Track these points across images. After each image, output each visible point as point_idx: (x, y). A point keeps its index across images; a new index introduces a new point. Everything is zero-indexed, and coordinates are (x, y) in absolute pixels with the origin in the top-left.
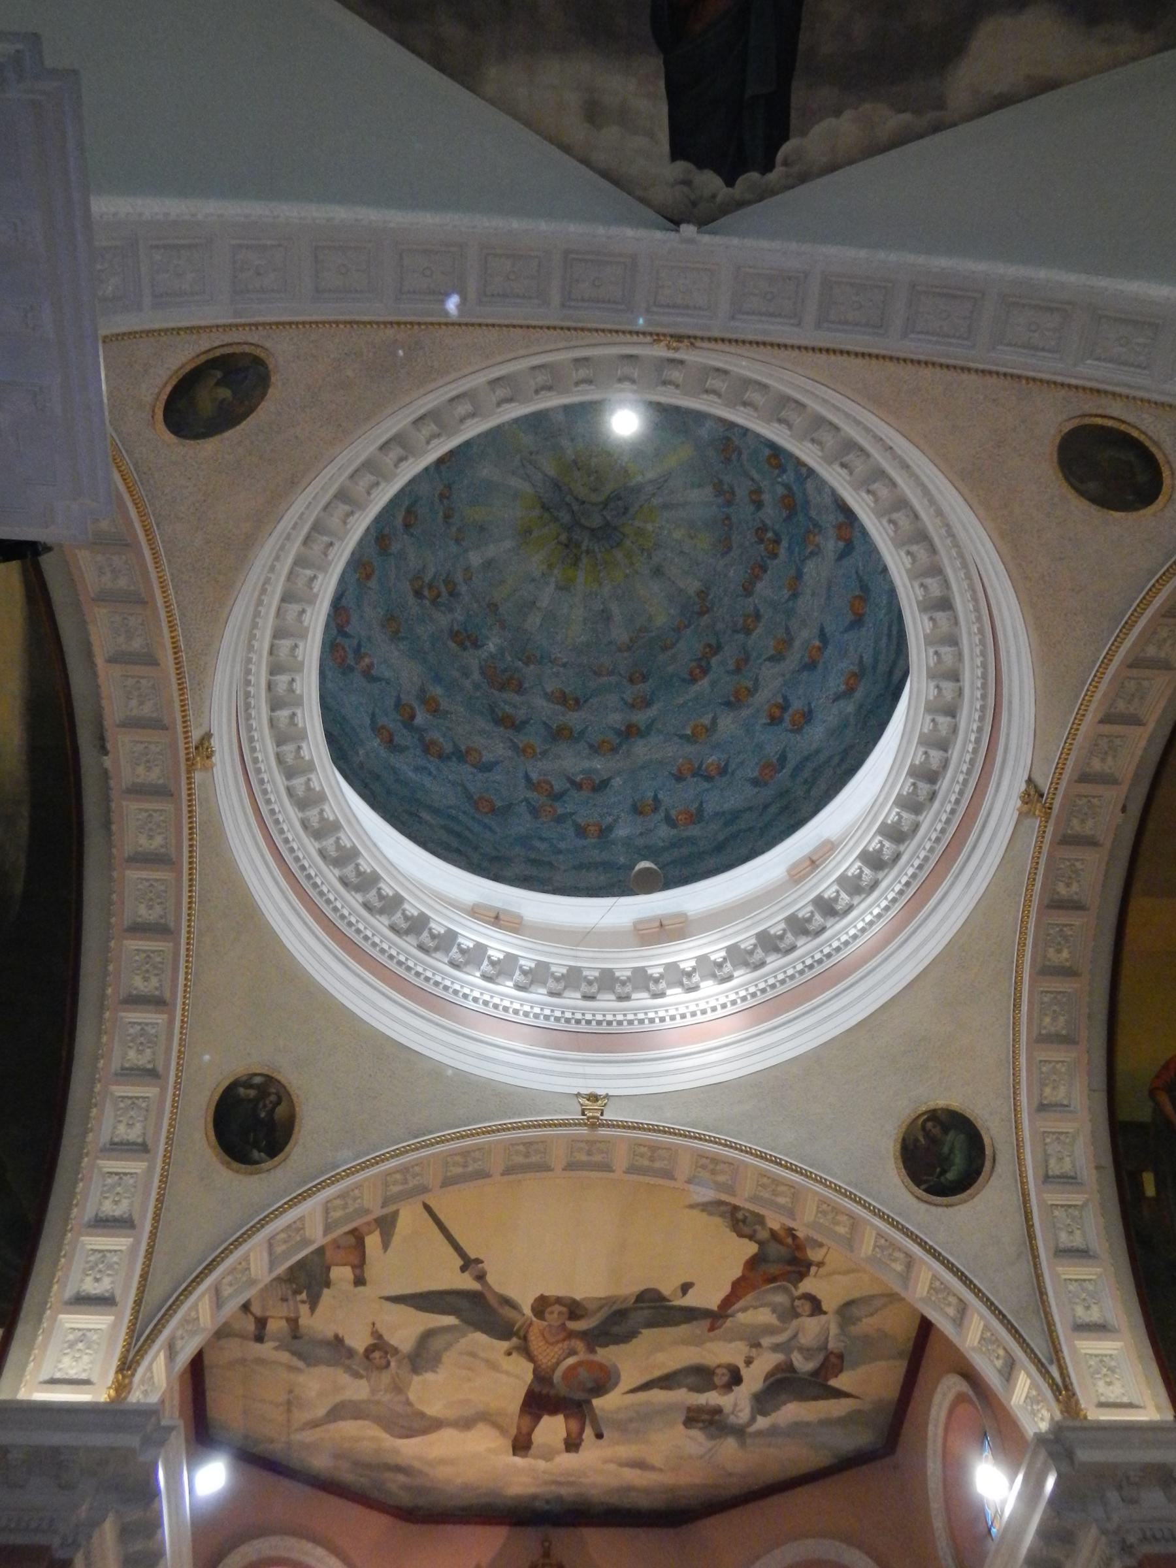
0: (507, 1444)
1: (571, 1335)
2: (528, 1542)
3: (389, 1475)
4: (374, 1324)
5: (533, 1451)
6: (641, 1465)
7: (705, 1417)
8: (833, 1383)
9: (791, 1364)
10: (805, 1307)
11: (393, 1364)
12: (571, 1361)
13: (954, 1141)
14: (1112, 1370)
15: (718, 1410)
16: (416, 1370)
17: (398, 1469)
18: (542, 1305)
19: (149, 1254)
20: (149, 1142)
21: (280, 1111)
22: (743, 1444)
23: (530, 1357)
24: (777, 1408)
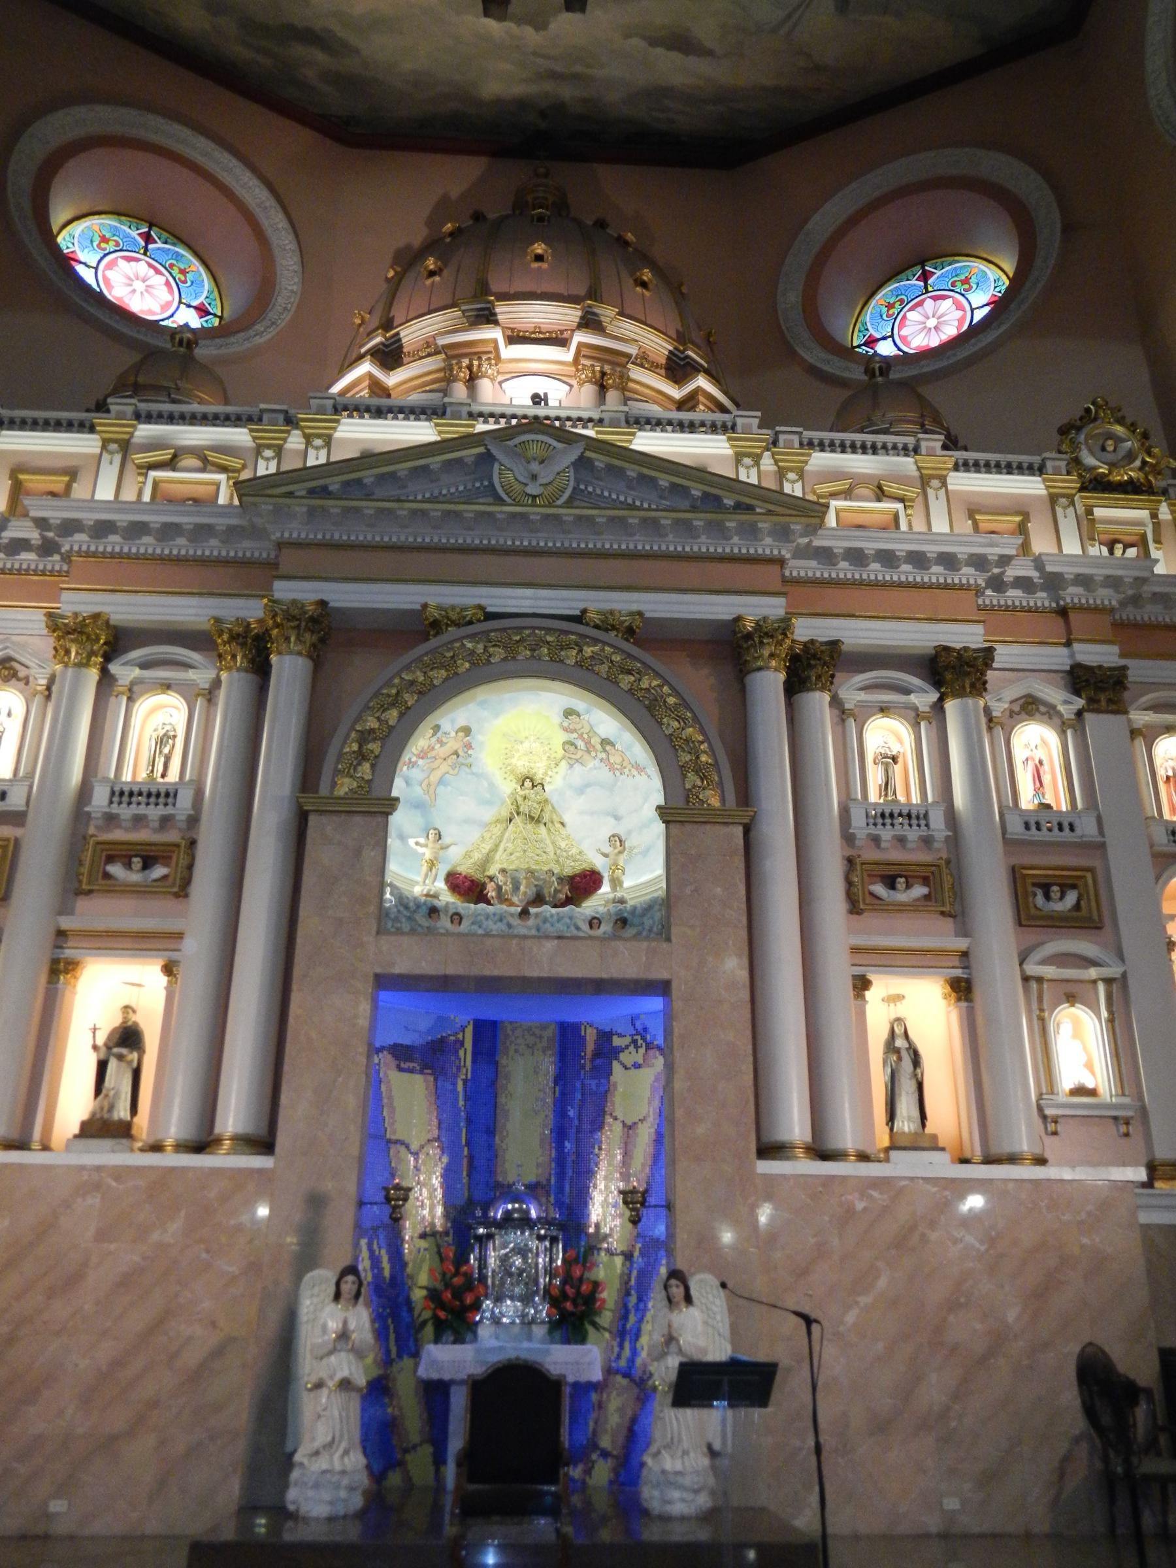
3: (299, 50)
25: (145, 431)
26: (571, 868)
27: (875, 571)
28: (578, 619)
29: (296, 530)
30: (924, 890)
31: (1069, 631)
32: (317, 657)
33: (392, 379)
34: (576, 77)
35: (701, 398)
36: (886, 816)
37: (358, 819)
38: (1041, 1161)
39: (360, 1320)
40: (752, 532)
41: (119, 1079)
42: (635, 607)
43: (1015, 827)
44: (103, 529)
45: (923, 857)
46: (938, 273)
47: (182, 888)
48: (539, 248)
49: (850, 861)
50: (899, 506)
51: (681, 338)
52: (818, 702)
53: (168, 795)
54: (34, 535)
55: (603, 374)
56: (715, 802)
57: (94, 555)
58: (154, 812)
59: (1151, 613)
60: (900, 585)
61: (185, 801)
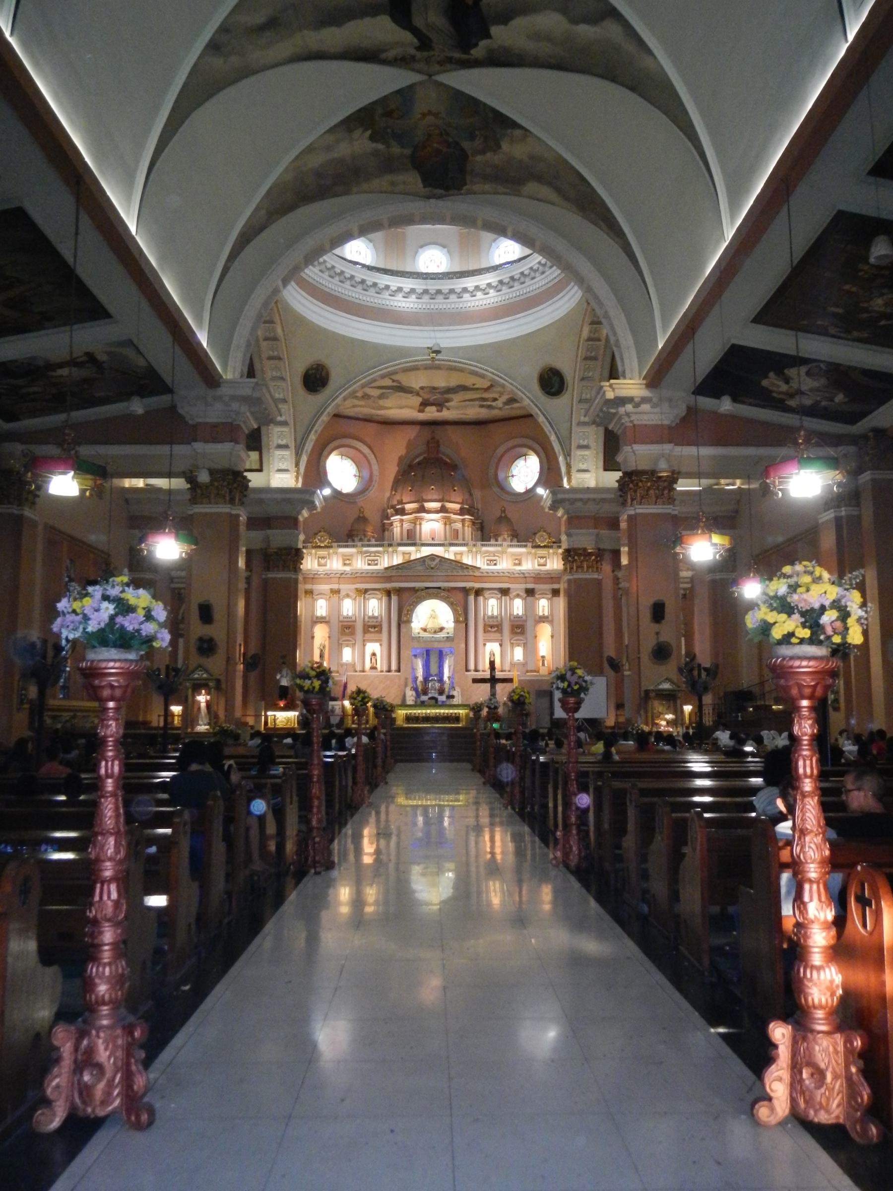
6: (465, 414)
13: (555, 379)
14: (586, 460)
18: (422, 388)
19: (295, 431)
20: (286, 398)
21: (324, 373)
25: (365, 549)
26: (440, 626)
27: (491, 574)
28: (439, 588)
29: (393, 574)
32: (398, 595)
33: (404, 517)
36: (492, 617)
38: (509, 671)
39: (414, 693)
40: (468, 572)
41: (373, 660)
43: (512, 618)
44: (362, 573)
45: (496, 623)
47: (380, 631)
49: (485, 625)
51: (462, 503)
52: (481, 599)
53: (376, 618)
58: (375, 620)
59: (542, 576)
61: (379, 618)
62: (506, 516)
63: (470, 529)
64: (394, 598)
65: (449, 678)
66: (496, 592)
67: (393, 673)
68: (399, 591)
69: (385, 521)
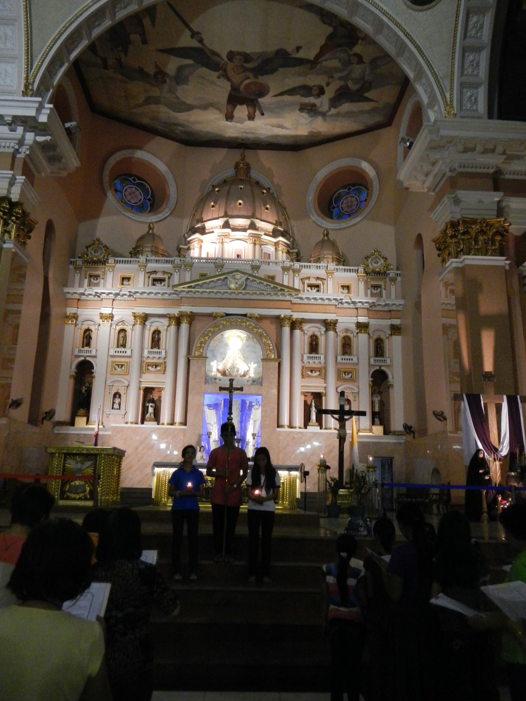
0: (222, 116)
1: (246, 70)
2: (235, 155)
4: (155, 62)
5: (234, 119)
7: (309, 108)
8: (366, 95)
9: (347, 86)
10: (355, 59)
11: (168, 81)
12: (247, 81)
15: (314, 105)
16: (178, 83)
17: (178, 125)
18: (231, 55)
22: (325, 120)
23: (229, 79)
24: (340, 105)
27: (313, 301)
28: (245, 315)
30: (319, 373)
31: (358, 314)
32: (190, 324)
34: (252, 133)
35: (280, 242)
37: (200, 361)
42: (259, 312)
46: (353, 188)
48: (241, 201)
49: (303, 367)
50: (321, 282)
51: (276, 224)
54: (128, 293)
55: (255, 240)
56: (273, 357)
57: (141, 298)
58: (157, 356)
60: (318, 304)
62: (329, 239)
63: (285, 254)
64: (184, 326)
65: (254, 435)
66: (318, 325)
67: (177, 426)
68: (192, 317)
69: (181, 246)
